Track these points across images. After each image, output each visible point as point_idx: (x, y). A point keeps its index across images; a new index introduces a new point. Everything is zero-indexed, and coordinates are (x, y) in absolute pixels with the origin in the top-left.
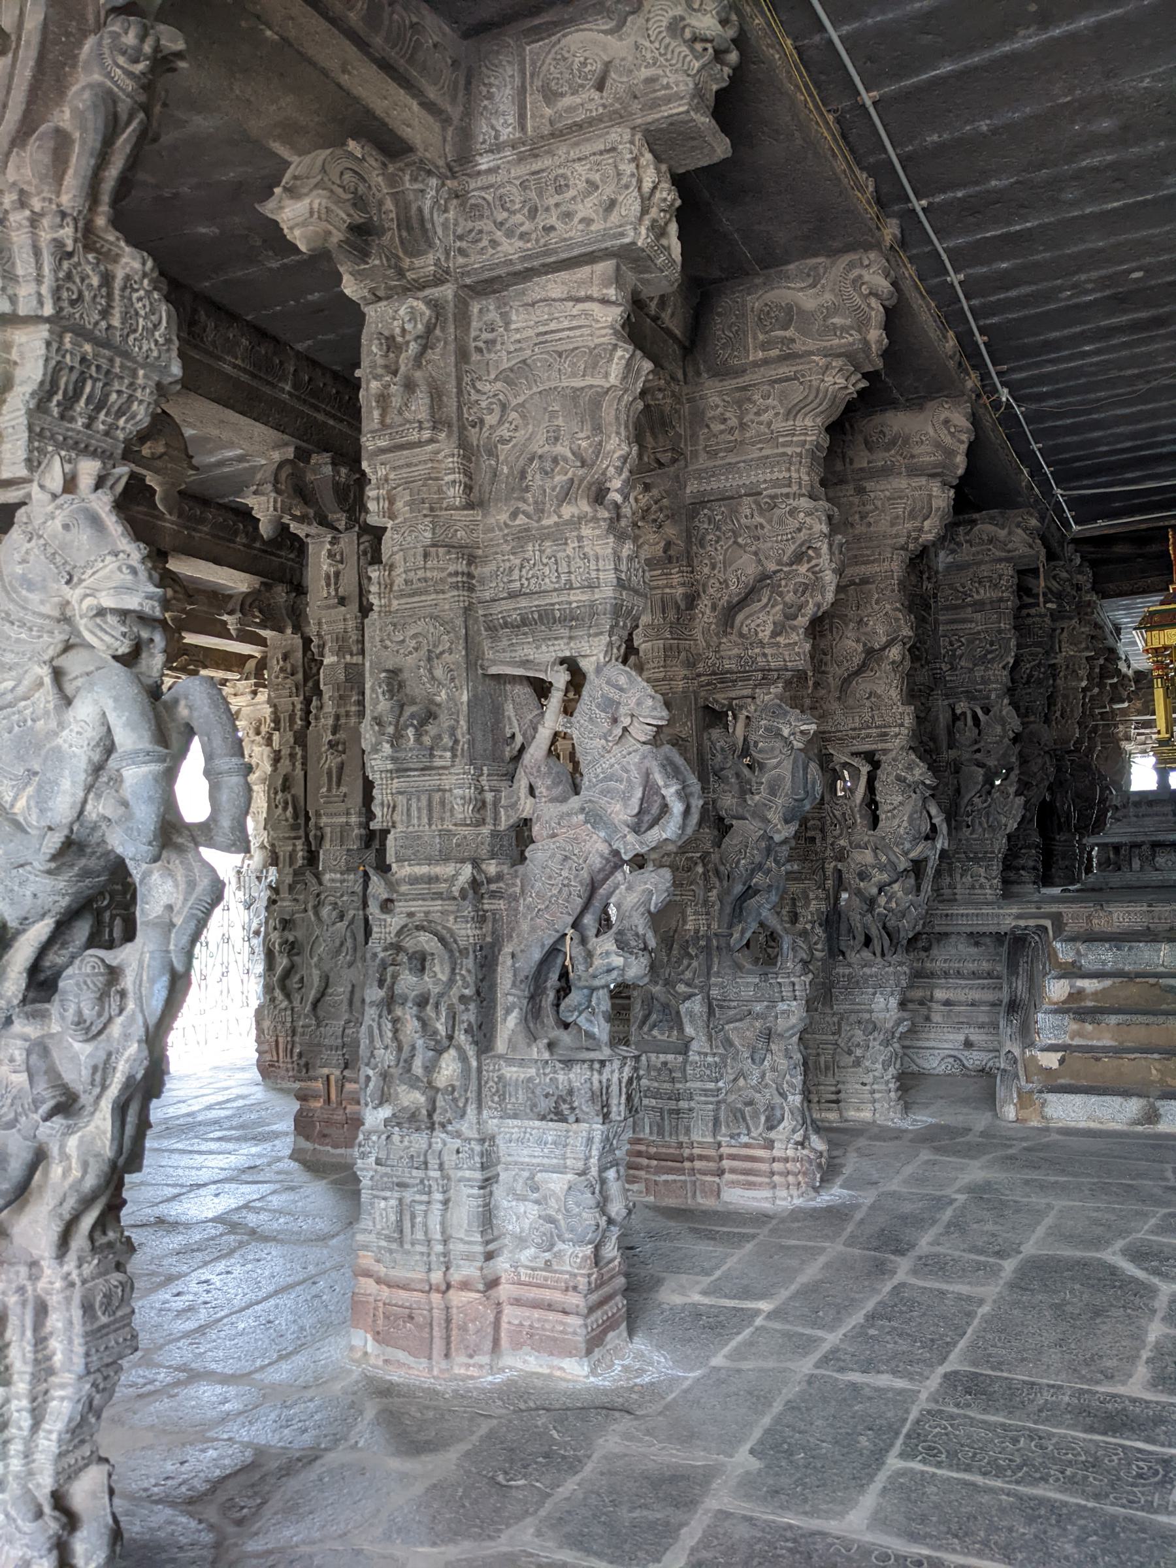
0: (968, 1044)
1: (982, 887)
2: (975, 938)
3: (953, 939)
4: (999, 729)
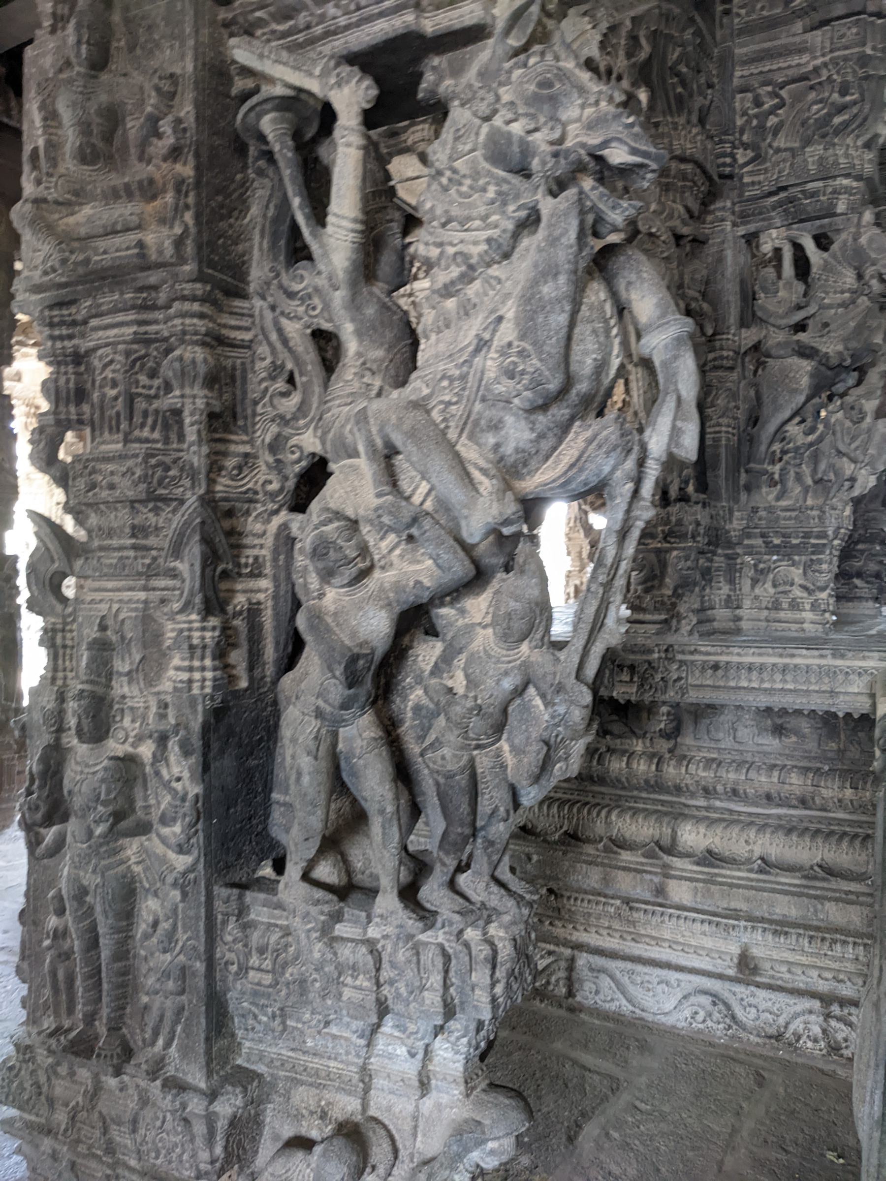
0: (747, 968)
1: (795, 605)
2: (777, 721)
3: (726, 718)
4: (849, 278)
